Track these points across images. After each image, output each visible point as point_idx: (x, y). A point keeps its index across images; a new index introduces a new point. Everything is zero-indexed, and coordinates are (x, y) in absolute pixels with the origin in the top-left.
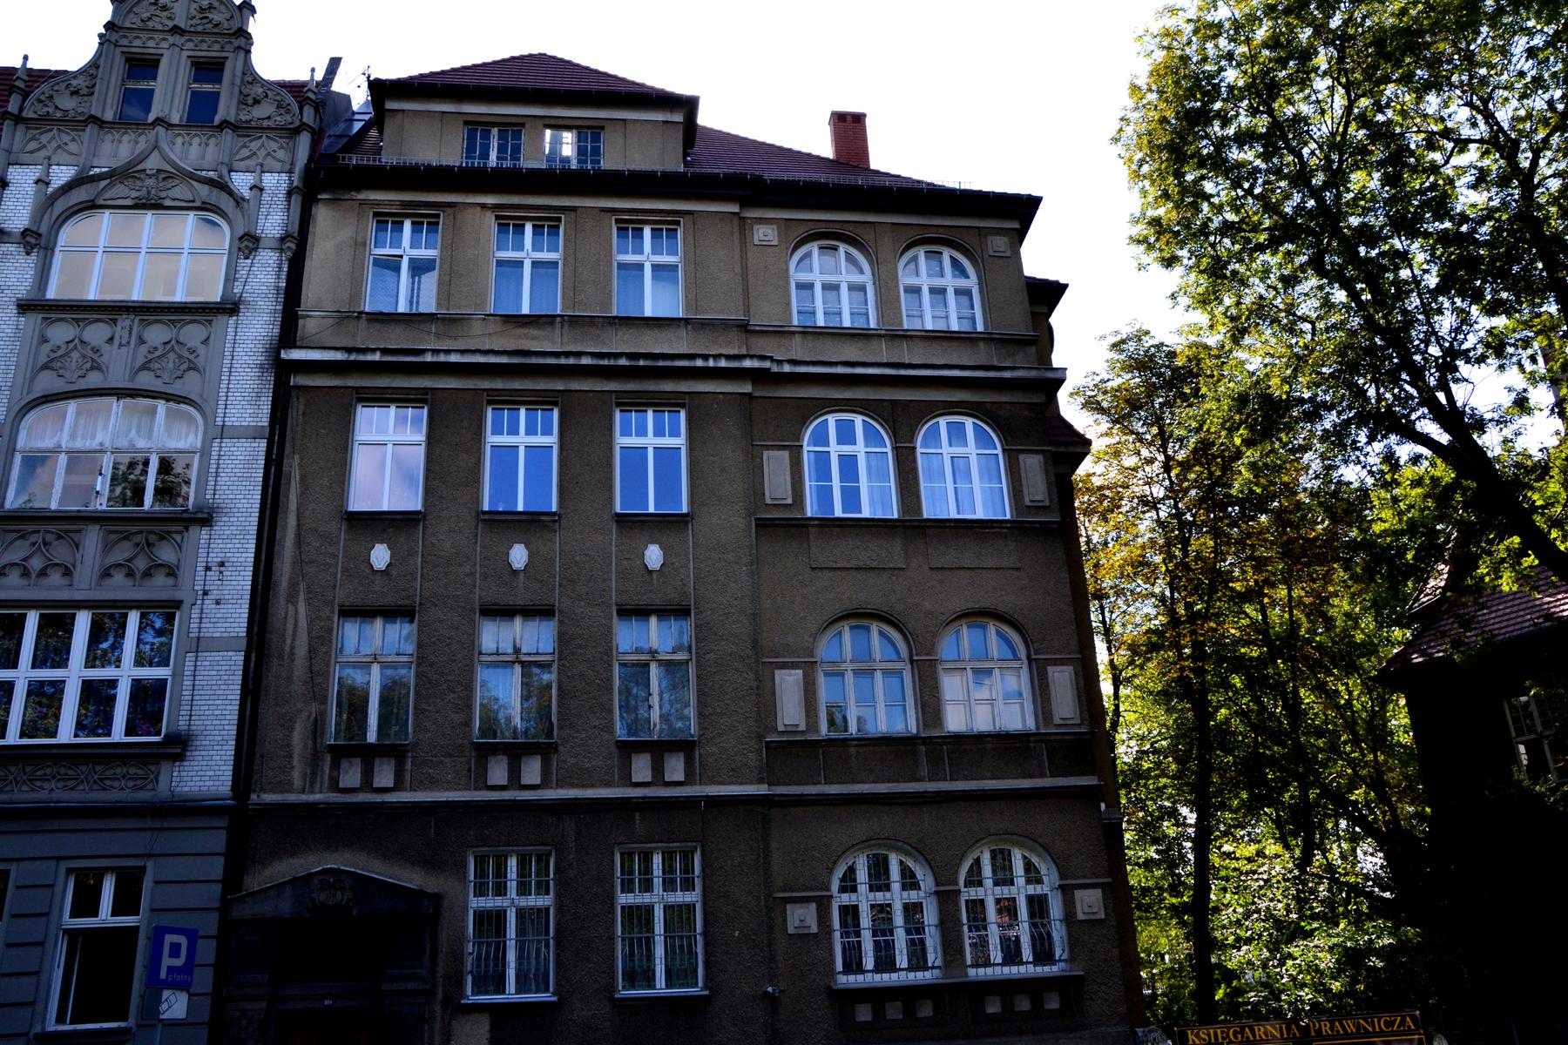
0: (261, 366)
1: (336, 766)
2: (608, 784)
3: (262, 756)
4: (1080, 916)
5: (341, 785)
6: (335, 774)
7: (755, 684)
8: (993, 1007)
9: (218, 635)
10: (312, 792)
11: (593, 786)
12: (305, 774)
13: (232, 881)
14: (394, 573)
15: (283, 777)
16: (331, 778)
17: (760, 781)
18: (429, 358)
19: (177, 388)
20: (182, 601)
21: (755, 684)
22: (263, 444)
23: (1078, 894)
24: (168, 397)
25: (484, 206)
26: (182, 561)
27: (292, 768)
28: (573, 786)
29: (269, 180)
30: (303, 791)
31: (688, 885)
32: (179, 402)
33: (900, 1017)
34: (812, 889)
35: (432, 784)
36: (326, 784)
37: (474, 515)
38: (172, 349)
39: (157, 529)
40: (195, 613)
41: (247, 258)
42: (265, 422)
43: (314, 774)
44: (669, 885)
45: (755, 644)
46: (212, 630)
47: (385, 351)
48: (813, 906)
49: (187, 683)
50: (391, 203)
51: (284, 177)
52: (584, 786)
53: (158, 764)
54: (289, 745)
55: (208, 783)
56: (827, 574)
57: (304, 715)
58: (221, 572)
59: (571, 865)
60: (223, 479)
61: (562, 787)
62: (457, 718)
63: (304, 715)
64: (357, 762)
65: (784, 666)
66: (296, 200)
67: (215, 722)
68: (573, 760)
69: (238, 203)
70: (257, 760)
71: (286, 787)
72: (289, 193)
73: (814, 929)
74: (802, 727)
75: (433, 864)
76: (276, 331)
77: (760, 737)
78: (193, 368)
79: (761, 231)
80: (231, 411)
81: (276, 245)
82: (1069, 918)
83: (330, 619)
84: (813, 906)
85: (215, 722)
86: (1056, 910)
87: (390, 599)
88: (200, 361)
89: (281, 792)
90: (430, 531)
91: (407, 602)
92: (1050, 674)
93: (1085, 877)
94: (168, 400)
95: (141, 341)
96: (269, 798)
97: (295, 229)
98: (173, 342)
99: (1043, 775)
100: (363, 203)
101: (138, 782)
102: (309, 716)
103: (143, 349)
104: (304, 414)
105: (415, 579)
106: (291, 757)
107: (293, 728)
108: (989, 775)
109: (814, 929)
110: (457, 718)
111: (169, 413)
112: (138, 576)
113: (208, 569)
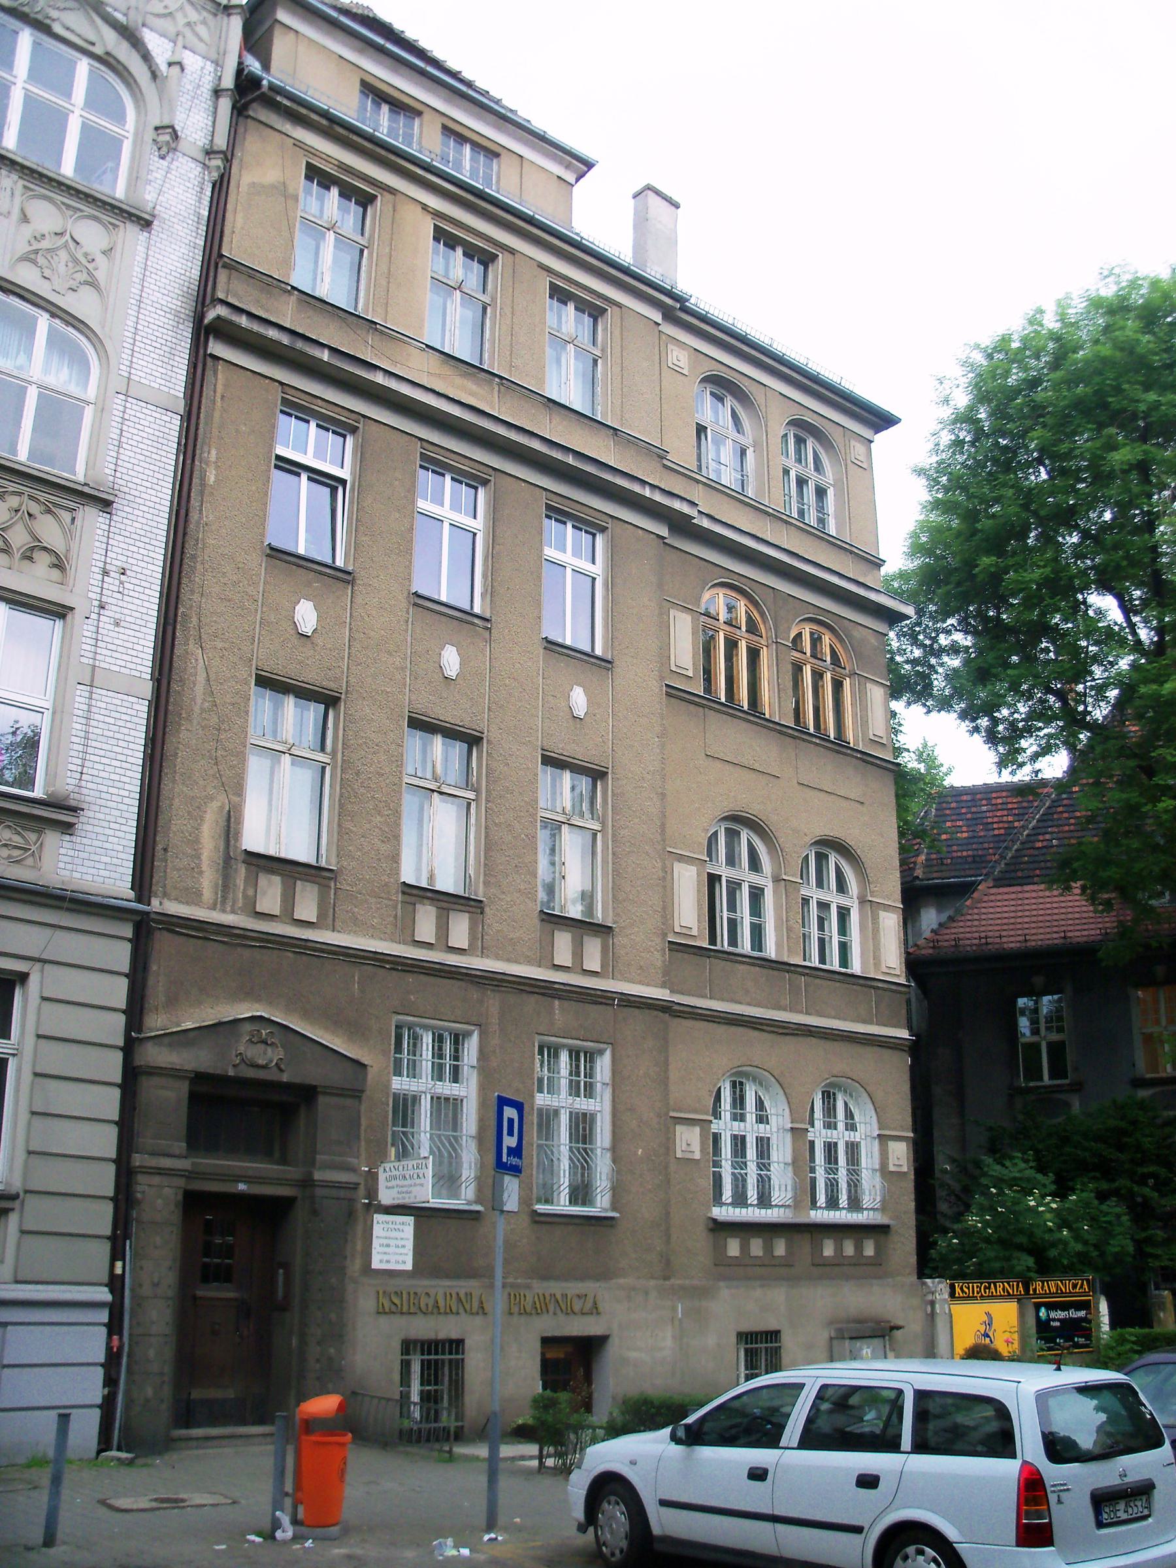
0: (177, 314)
1: (253, 882)
2: (529, 962)
3: (165, 850)
4: (892, 1168)
5: (258, 910)
6: (250, 892)
7: (661, 874)
8: (828, 1250)
9: (117, 669)
10: (224, 911)
11: (517, 962)
12: (216, 885)
13: (135, 1011)
14: (320, 641)
15: (190, 883)
16: (245, 896)
17: (663, 985)
18: (379, 378)
19: (66, 302)
20: (72, 609)
21: (661, 874)
22: (177, 420)
23: (892, 1145)
24: (55, 311)
25: (425, 207)
26: (73, 554)
27: (201, 873)
28: (497, 957)
29: (192, 62)
30: (213, 907)
31: (590, 1091)
32: (68, 323)
33: (761, 1254)
34: (695, 1111)
35: (357, 925)
36: (240, 904)
37: (406, 594)
38: (66, 246)
39: (42, 496)
40: (88, 630)
41: (163, 158)
42: (179, 390)
43: (226, 887)
44: (574, 1089)
45: (663, 826)
46: (106, 661)
47: (334, 351)
48: (697, 1129)
49: (77, 726)
50: (327, 158)
51: (210, 67)
52: (509, 960)
53: (40, 832)
54: (197, 841)
55: (102, 873)
56: (719, 764)
57: (215, 805)
58: (122, 583)
59: (494, 1052)
60: (126, 454)
61: (488, 957)
62: (385, 848)
63: (215, 805)
64: (277, 880)
65: (682, 858)
66: (225, 104)
67: (111, 790)
68: (496, 926)
69: (154, 75)
70: (159, 853)
71: (193, 896)
72: (217, 93)
73: (697, 1156)
74: (695, 932)
75: (355, 1029)
76: (196, 273)
77: (665, 935)
78: (93, 284)
79: (675, 354)
80: (139, 362)
81: (201, 157)
82: (884, 1170)
83: (247, 683)
84: (697, 1129)
85: (111, 790)
86: (869, 1158)
87: (312, 676)
88: (101, 276)
89: (187, 903)
90: (359, 600)
91: (332, 685)
92: (881, 919)
93: (894, 1129)
94: (53, 315)
95: (25, 219)
96: (174, 908)
97: (221, 142)
98: (68, 237)
99: (871, 1023)
100: (298, 144)
101: (16, 853)
102: (222, 808)
103: (27, 231)
104: (223, 397)
105: (343, 658)
106: (199, 857)
107: (202, 819)
108: (833, 1013)
109: (697, 1156)
110: (385, 848)
111: (52, 334)
112: (17, 556)
113: (105, 573)
